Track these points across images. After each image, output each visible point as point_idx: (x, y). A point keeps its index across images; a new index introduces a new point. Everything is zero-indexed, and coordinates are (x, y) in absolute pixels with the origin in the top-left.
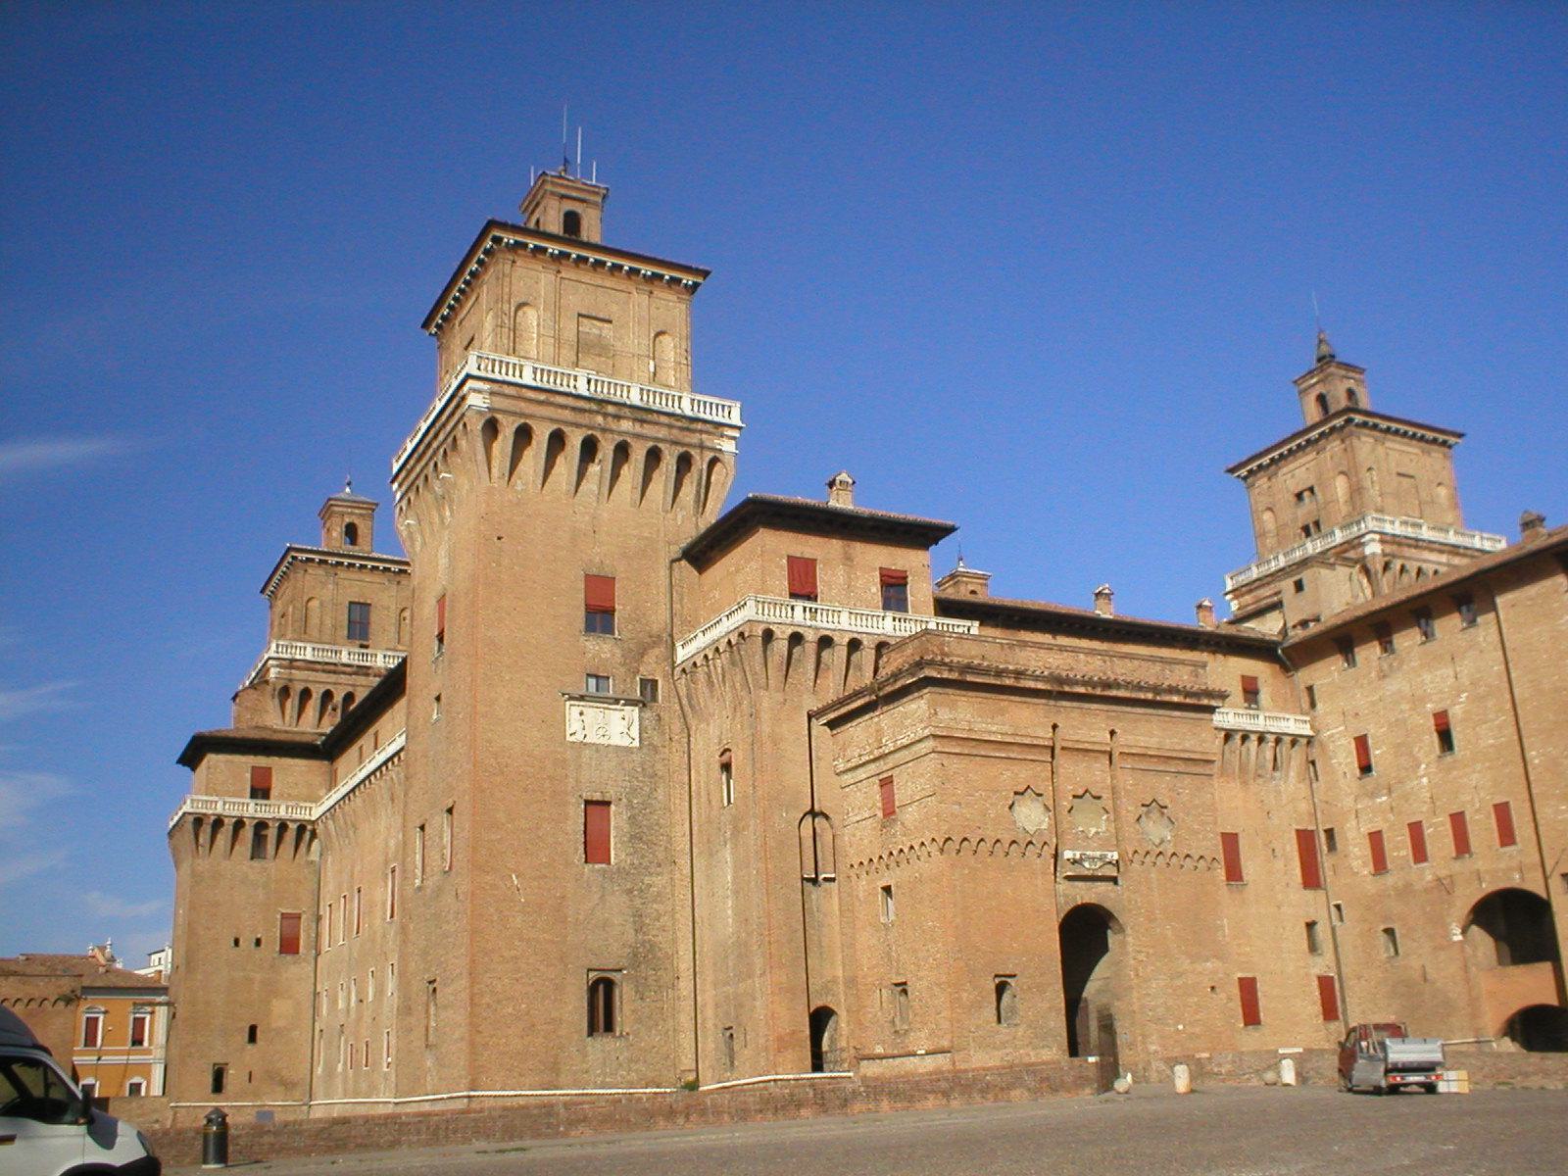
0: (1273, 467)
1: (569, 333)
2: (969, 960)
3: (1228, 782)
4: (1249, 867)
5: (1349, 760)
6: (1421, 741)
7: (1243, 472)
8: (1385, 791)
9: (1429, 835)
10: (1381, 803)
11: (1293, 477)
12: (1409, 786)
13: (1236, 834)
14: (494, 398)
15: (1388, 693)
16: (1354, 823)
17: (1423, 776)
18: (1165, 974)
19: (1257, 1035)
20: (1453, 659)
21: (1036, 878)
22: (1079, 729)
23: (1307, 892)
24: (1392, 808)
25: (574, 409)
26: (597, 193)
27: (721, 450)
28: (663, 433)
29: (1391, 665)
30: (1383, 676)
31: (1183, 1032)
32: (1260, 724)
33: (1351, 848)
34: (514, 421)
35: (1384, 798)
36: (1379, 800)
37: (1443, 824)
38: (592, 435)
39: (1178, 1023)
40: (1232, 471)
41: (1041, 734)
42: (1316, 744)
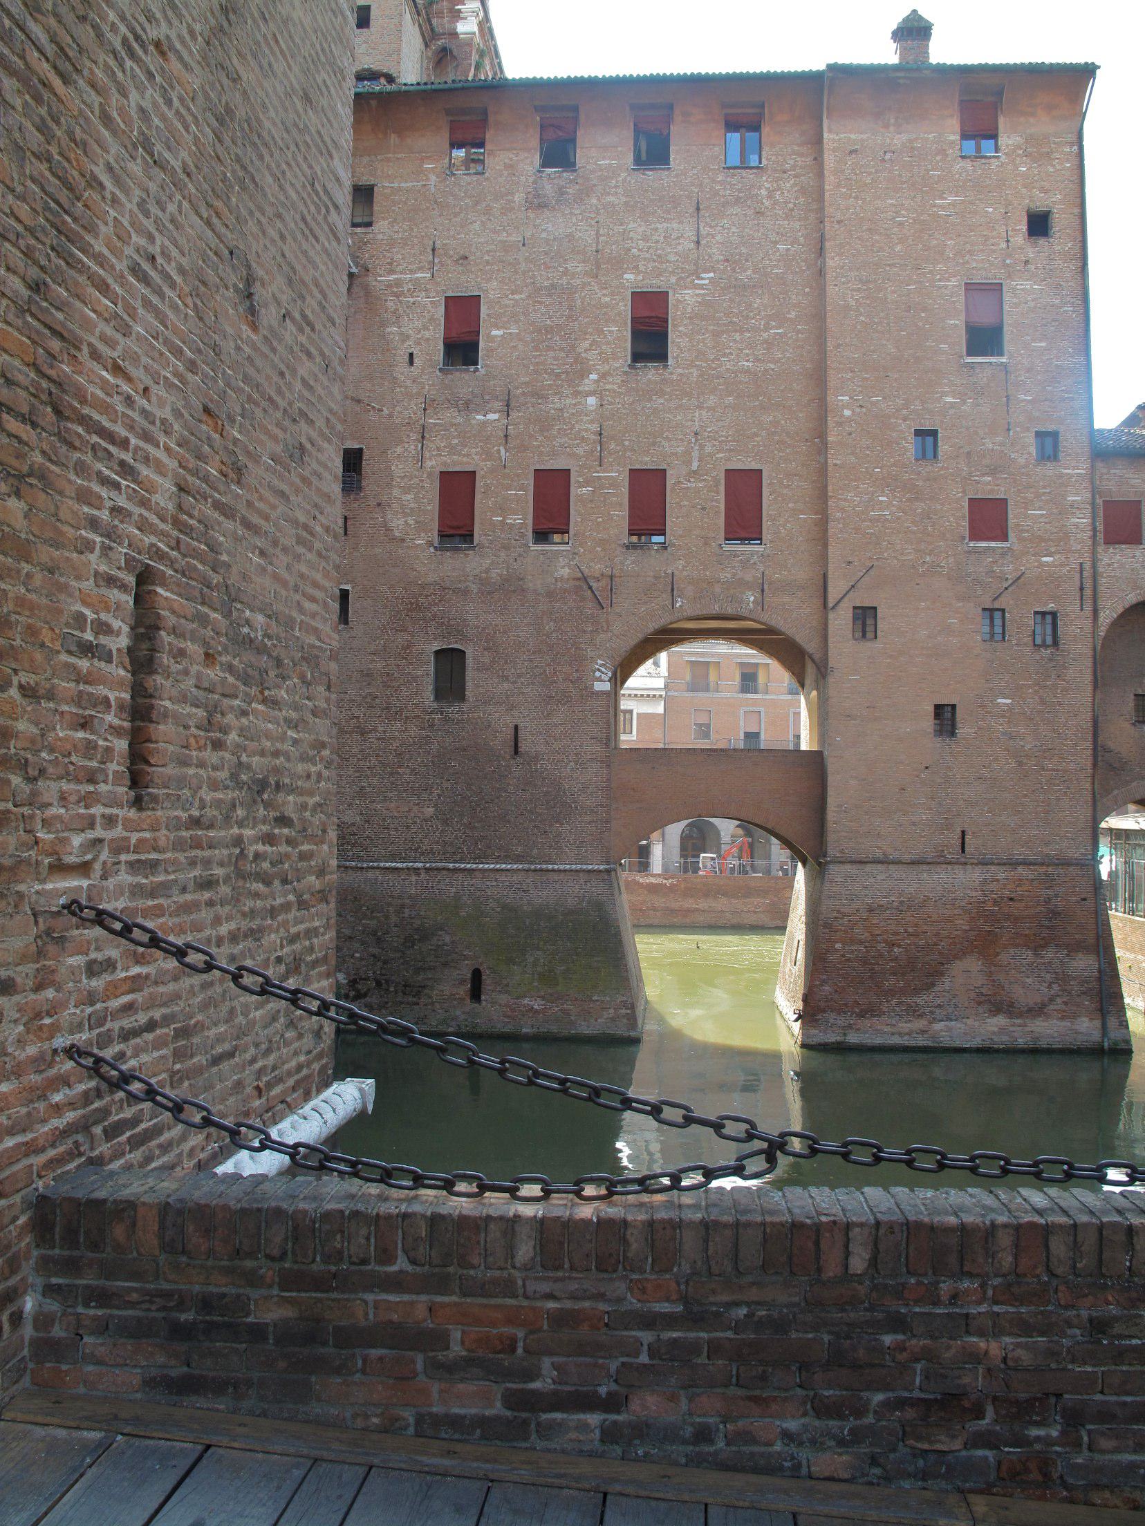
5: (427, 334)
6: (600, 332)
8: (497, 405)
9: (577, 495)
10: (484, 423)
12: (555, 403)
15: (544, 235)
16: (412, 448)
17: (592, 393)
20: (698, 209)
24: (506, 436)
29: (561, 192)
30: (537, 204)
33: (396, 492)
35: (492, 416)
36: (480, 417)
37: (614, 484)
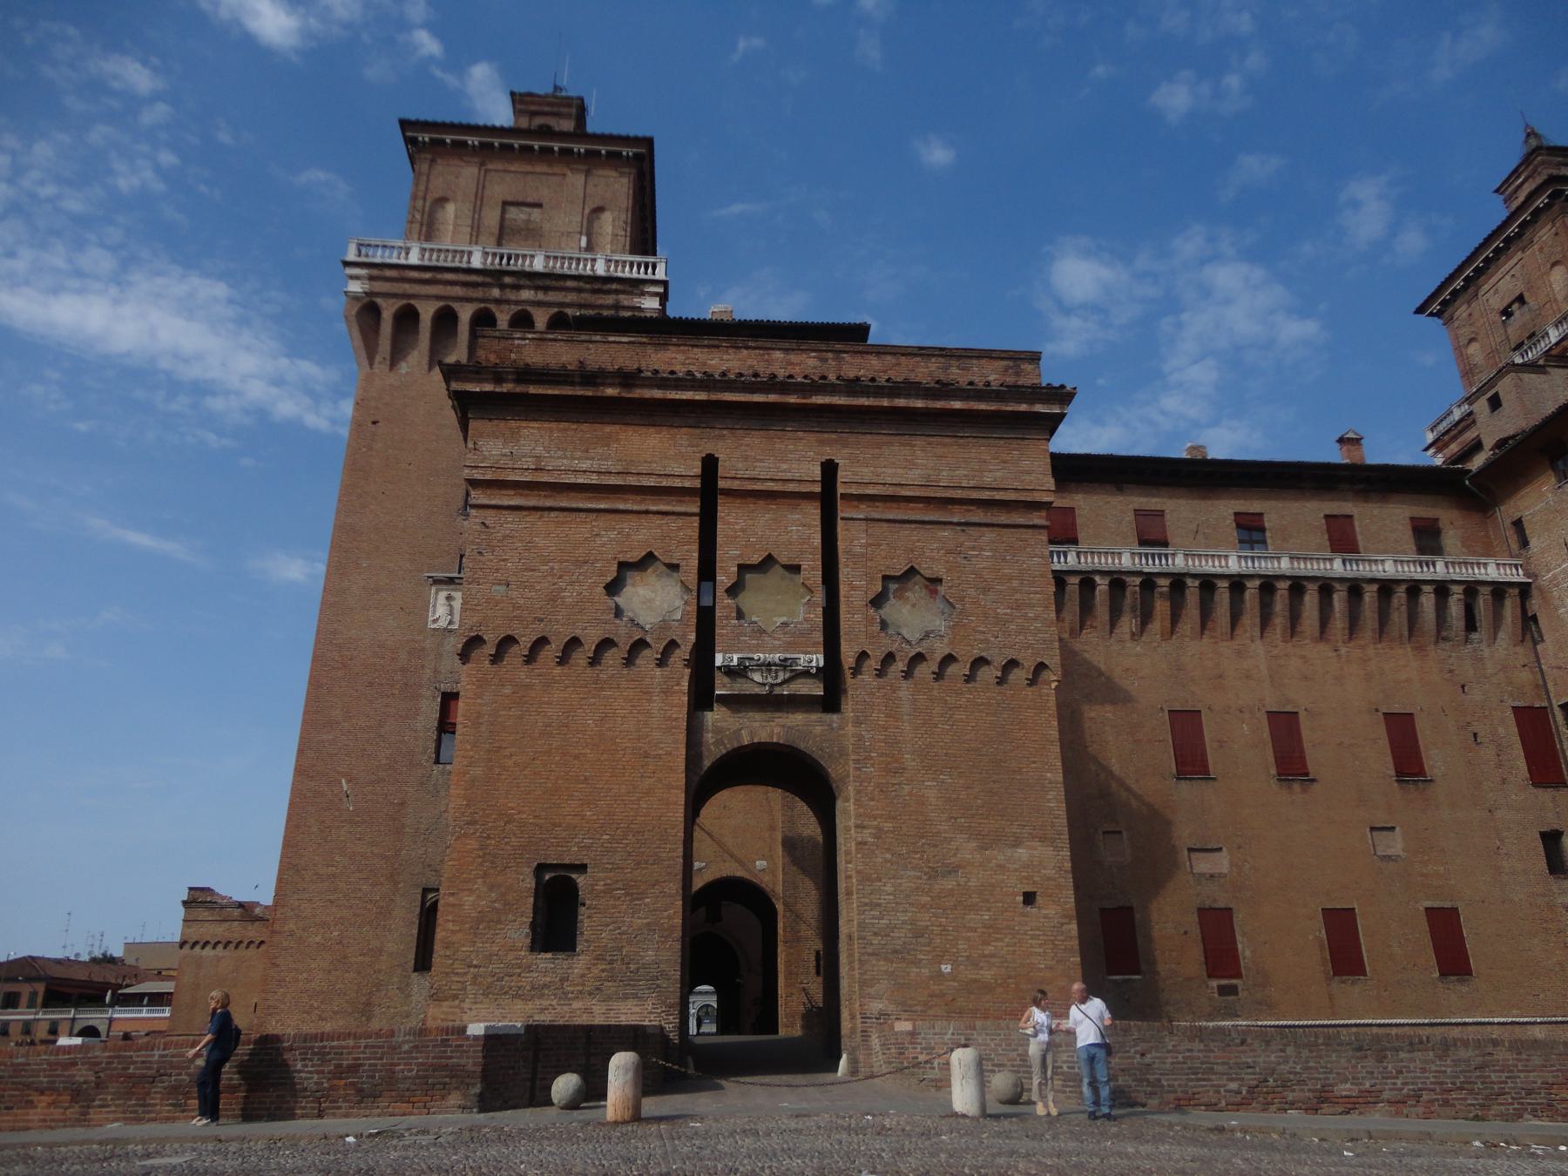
0: (1471, 290)
1: (491, 218)
2: (489, 837)
3: (1392, 649)
4: (1435, 759)
7: (1435, 307)
11: (1496, 292)
13: (1411, 714)
14: (374, 283)
18: (914, 868)
19: (1465, 989)
21: (650, 701)
22: (758, 460)
23: (1540, 792)
25: (465, 284)
26: (570, 106)
27: (640, 307)
28: (571, 297)
31: (953, 976)
32: (1440, 570)
34: (394, 304)
38: (486, 309)
39: (939, 959)
40: (1420, 310)
41: (677, 471)
42: (1535, 592)
